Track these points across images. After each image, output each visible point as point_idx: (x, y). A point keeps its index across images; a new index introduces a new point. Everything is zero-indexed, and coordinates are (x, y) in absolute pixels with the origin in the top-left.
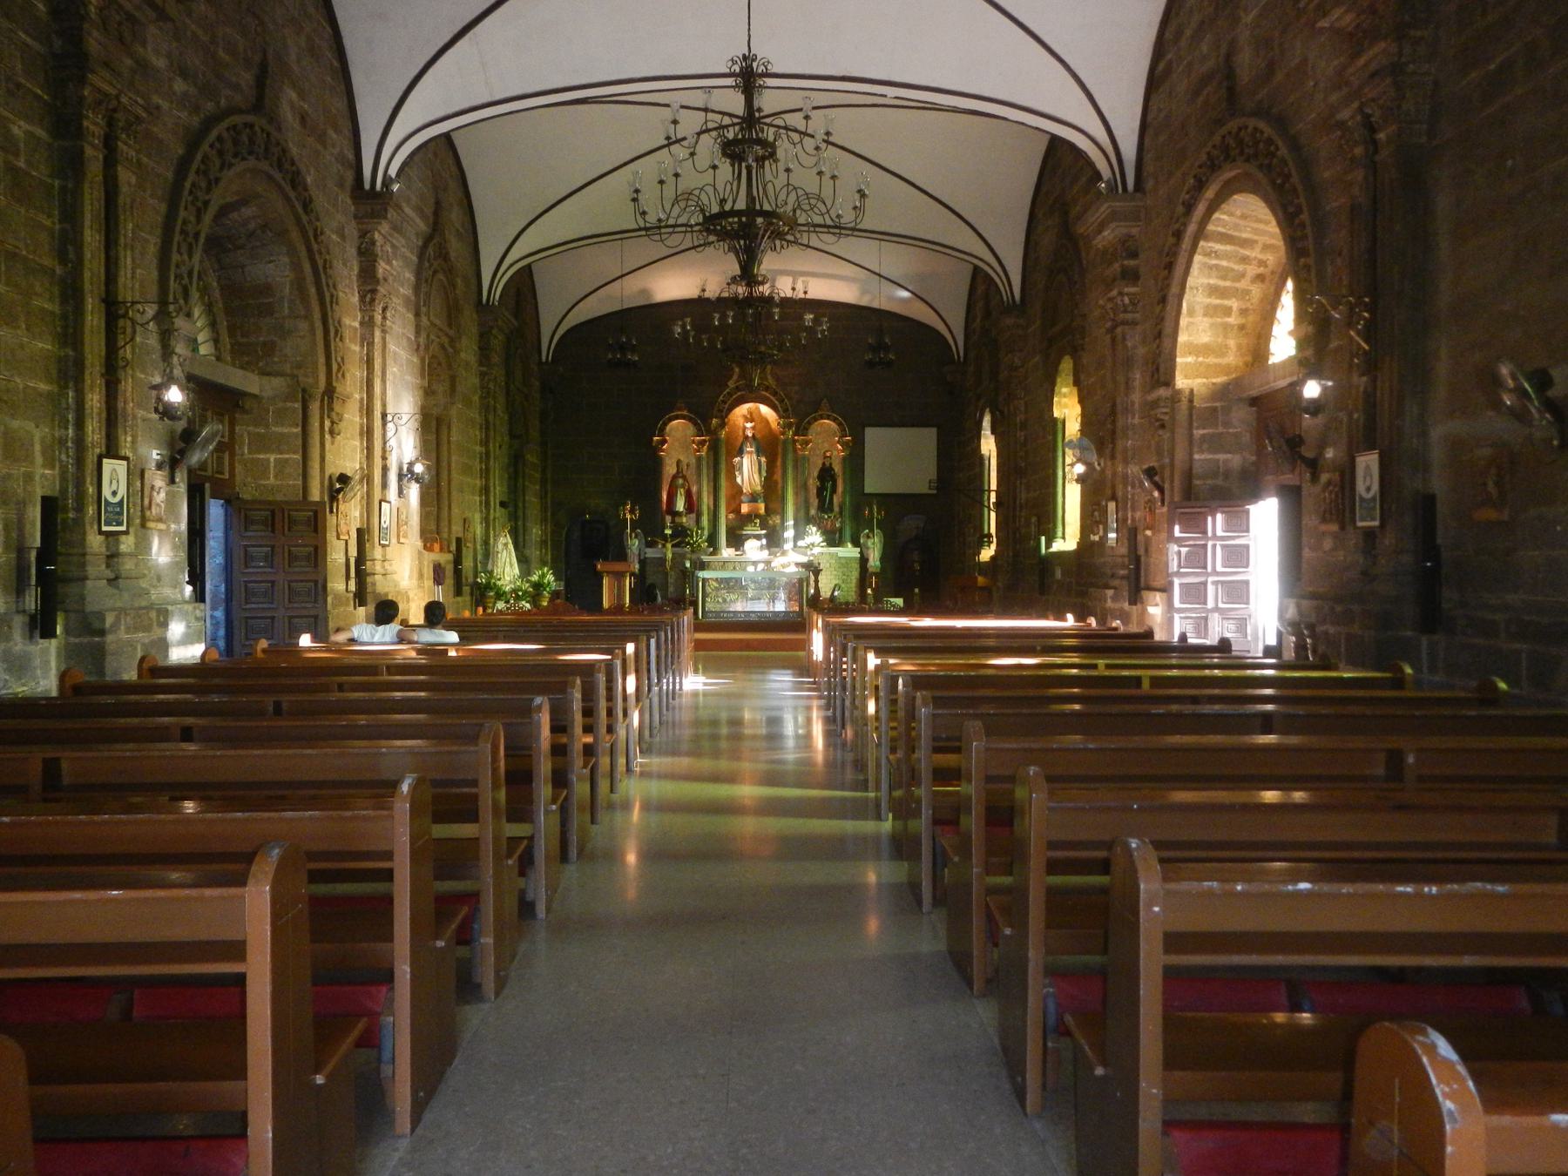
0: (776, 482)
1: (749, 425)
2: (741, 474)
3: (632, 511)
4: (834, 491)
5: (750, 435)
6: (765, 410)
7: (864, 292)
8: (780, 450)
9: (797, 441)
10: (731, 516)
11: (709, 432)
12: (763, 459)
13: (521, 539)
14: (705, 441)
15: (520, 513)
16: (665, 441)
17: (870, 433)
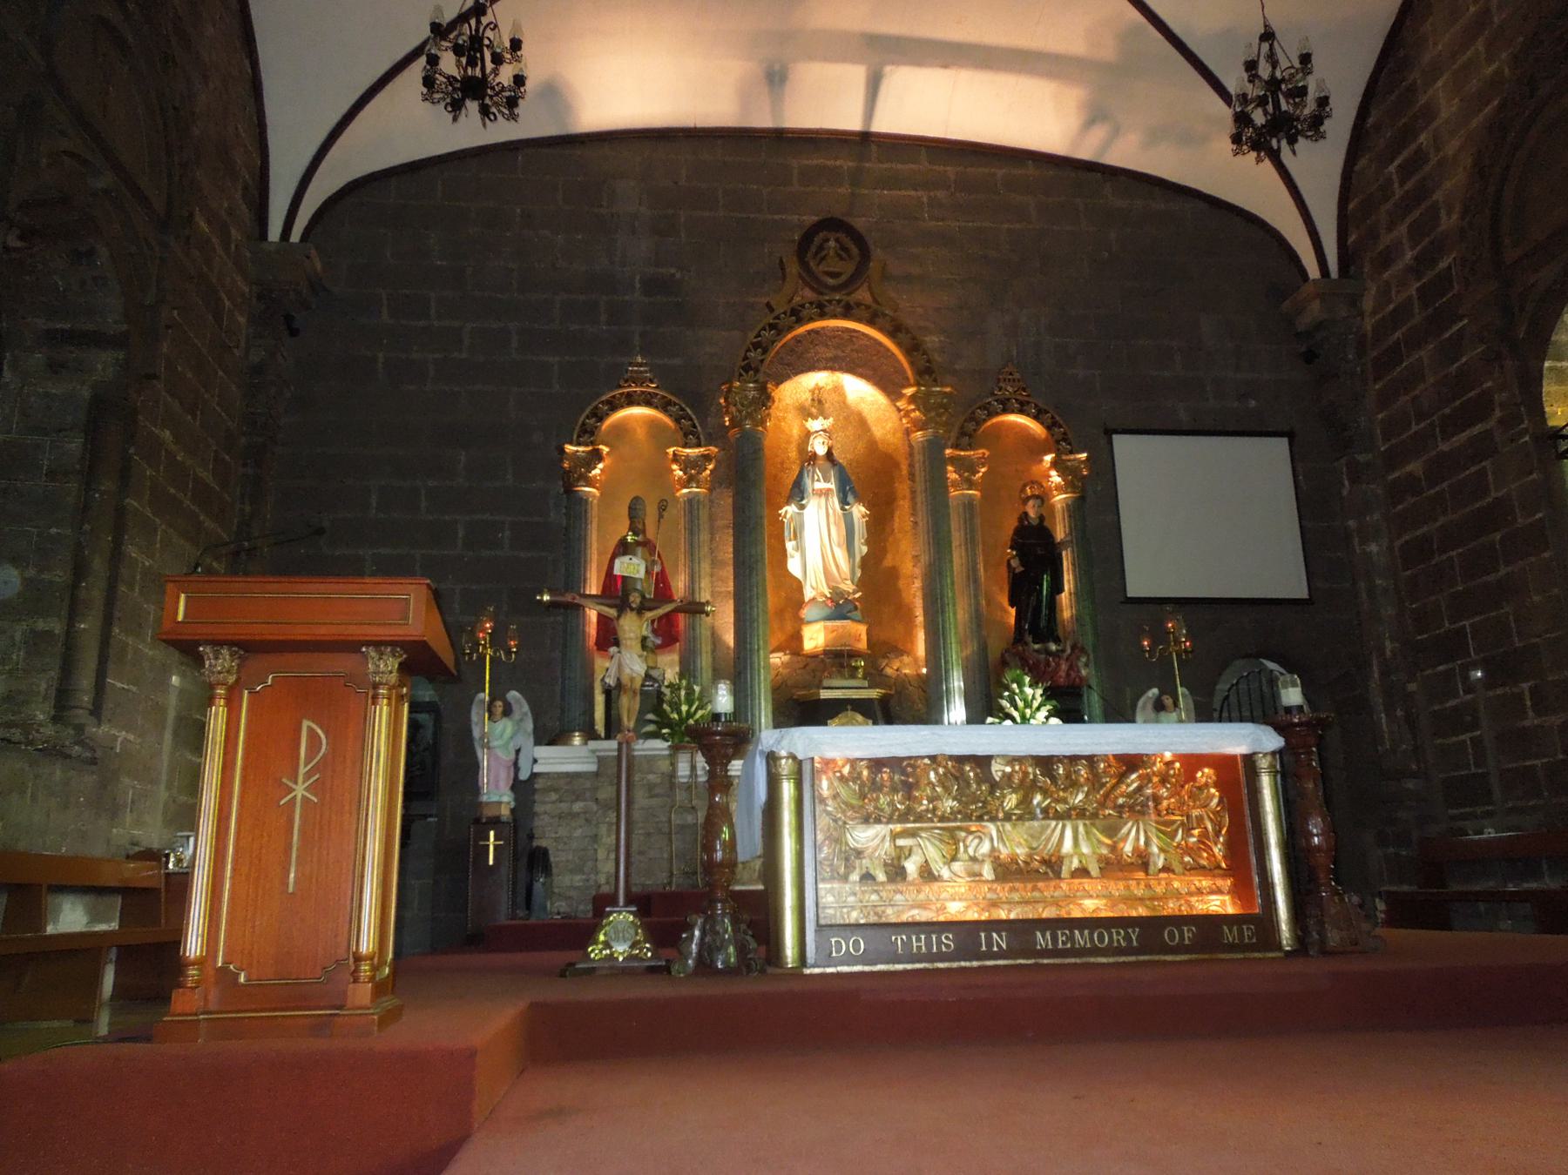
0: (893, 574)
1: (814, 425)
2: (800, 548)
3: (497, 640)
4: (1057, 587)
5: (821, 450)
6: (859, 391)
7: (1095, 115)
8: (903, 488)
9: (953, 460)
10: (777, 659)
11: (715, 436)
12: (859, 511)
13: (85, 681)
14: (707, 458)
15: (94, 591)
16: (596, 456)
17: (1124, 446)
